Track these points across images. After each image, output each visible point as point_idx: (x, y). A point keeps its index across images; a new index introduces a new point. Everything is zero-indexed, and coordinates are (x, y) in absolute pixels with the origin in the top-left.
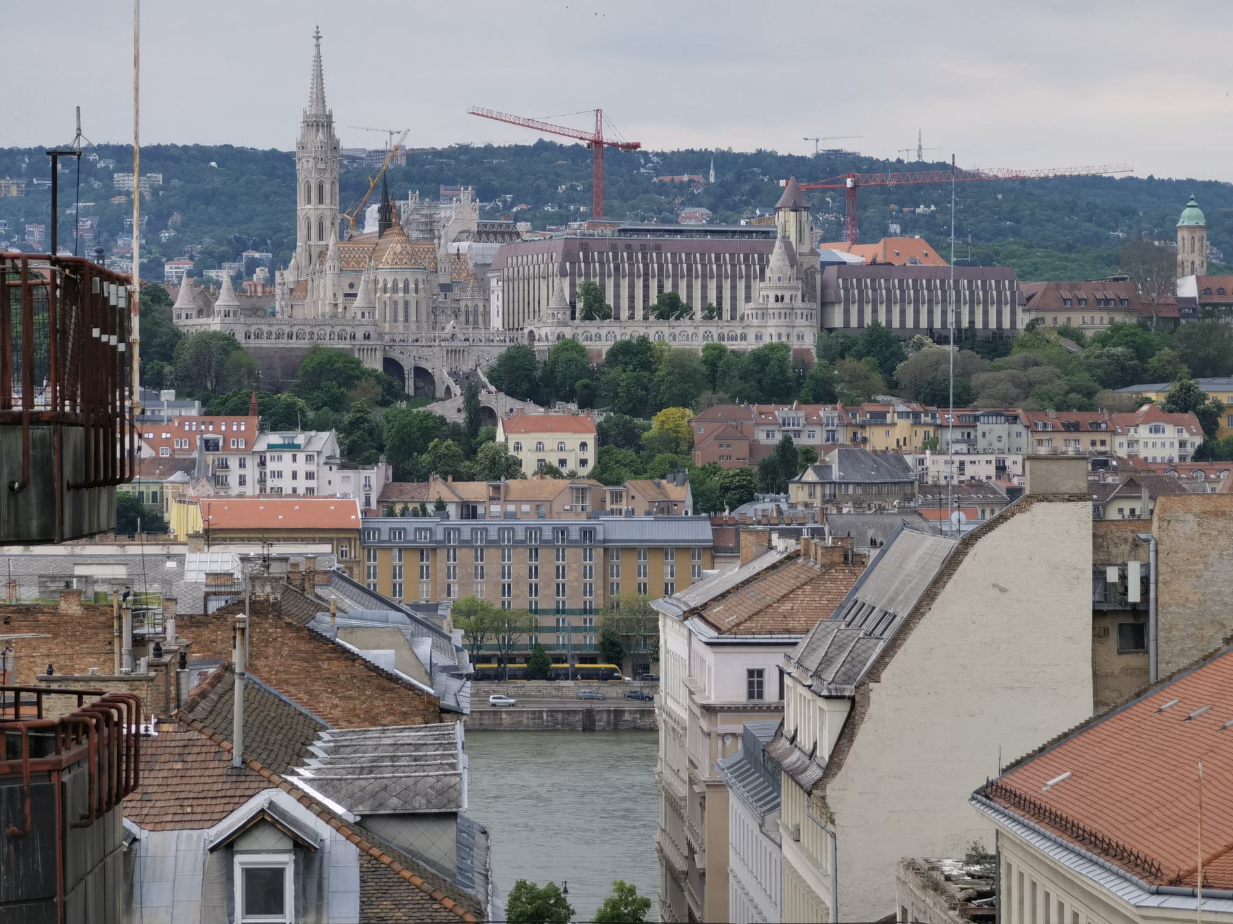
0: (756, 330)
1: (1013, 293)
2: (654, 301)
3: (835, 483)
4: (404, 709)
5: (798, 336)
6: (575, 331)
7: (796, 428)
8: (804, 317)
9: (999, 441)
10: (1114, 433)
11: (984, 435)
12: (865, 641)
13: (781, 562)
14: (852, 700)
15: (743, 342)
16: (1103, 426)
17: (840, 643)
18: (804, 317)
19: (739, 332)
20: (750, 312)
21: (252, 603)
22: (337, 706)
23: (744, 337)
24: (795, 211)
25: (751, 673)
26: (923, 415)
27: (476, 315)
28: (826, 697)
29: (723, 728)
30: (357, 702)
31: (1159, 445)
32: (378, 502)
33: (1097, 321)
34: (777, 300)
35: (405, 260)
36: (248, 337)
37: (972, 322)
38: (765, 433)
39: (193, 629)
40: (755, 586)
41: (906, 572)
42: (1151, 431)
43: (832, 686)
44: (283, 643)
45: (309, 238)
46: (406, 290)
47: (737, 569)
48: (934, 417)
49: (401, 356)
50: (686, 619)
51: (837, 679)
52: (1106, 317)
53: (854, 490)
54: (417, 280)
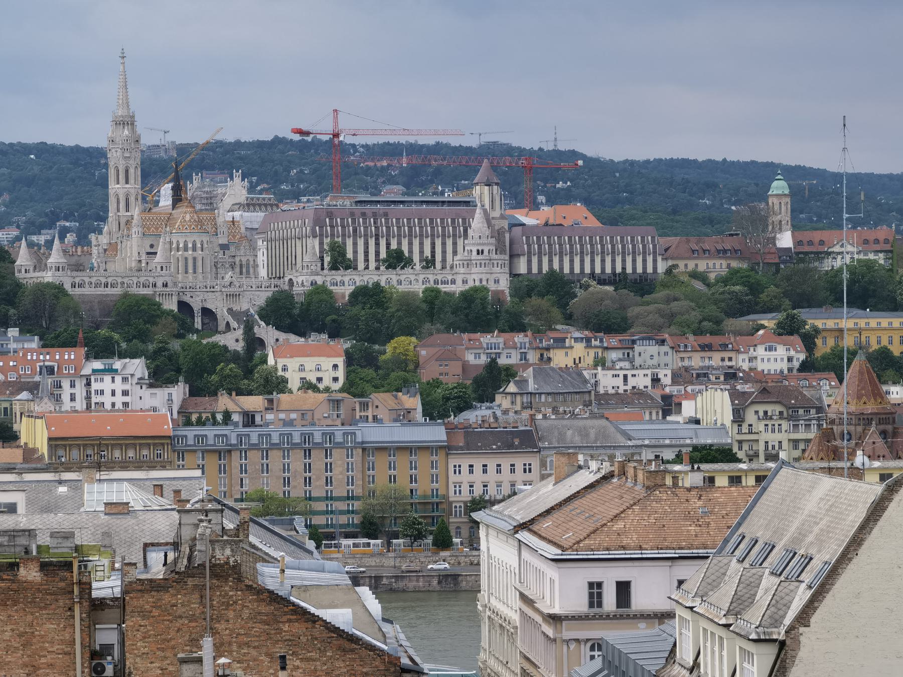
0: (464, 276)
1: (654, 246)
2: (383, 255)
3: (531, 393)
4: (364, 670)
5: (495, 280)
6: (324, 279)
7: (497, 351)
8: (499, 265)
9: (651, 359)
10: (738, 351)
12: (787, 584)
14: (782, 644)
16: (730, 346)
17: (748, 582)
18: (499, 265)
19: (450, 278)
22: (298, 667)
23: (453, 282)
24: (489, 185)
25: (591, 585)
26: (593, 340)
28: (755, 641)
29: (567, 634)
30: (318, 663)
31: (772, 360)
32: (179, 413)
33: (718, 266)
34: (478, 254)
35: (193, 226)
36: (73, 286)
37: (624, 268)
39: (153, 593)
40: (576, 503)
41: (806, 512)
42: (766, 350)
43: (760, 630)
44: (244, 606)
45: (118, 210)
46: (194, 249)
48: (601, 341)
49: (191, 299)
50: (516, 532)
51: (763, 623)
52: (724, 263)
53: (546, 398)
54: (202, 241)
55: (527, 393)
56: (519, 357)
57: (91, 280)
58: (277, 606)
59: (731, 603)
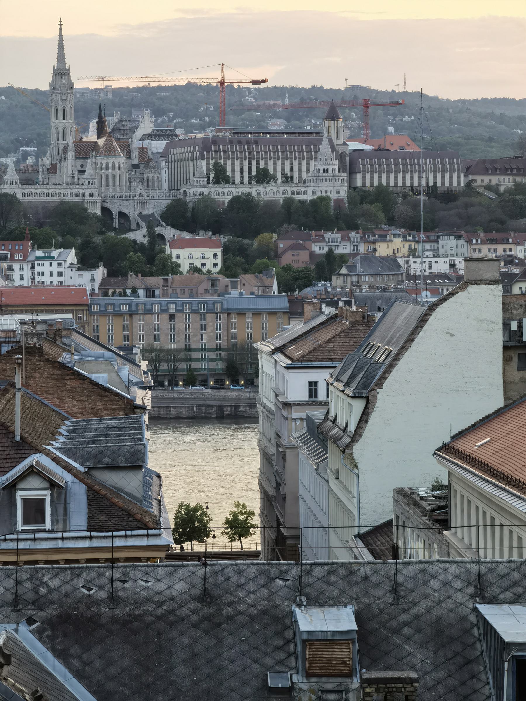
2: (254, 172)
3: (358, 275)
4: (113, 407)
5: (337, 192)
6: (210, 190)
7: (336, 244)
8: (340, 180)
9: (451, 250)
11: (443, 246)
12: (374, 365)
13: (327, 321)
15: (305, 196)
16: (510, 240)
17: (360, 367)
18: (340, 180)
19: (303, 189)
20: (309, 178)
21: (27, 348)
22: (75, 405)
23: (306, 193)
25: (310, 384)
26: (408, 236)
27: (153, 183)
28: (353, 397)
32: (99, 289)
35: (113, 151)
36: (24, 195)
37: (435, 183)
38: (318, 247)
41: (397, 325)
43: (356, 391)
44: (44, 371)
45: (58, 139)
46: (113, 168)
47: (302, 325)
53: (369, 278)
54: (119, 162)
55: (356, 275)
56: (352, 249)
57: (36, 191)
58: (63, 370)
59: (349, 378)
